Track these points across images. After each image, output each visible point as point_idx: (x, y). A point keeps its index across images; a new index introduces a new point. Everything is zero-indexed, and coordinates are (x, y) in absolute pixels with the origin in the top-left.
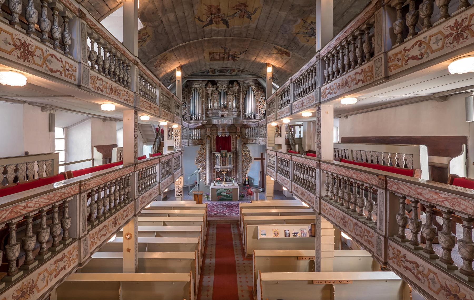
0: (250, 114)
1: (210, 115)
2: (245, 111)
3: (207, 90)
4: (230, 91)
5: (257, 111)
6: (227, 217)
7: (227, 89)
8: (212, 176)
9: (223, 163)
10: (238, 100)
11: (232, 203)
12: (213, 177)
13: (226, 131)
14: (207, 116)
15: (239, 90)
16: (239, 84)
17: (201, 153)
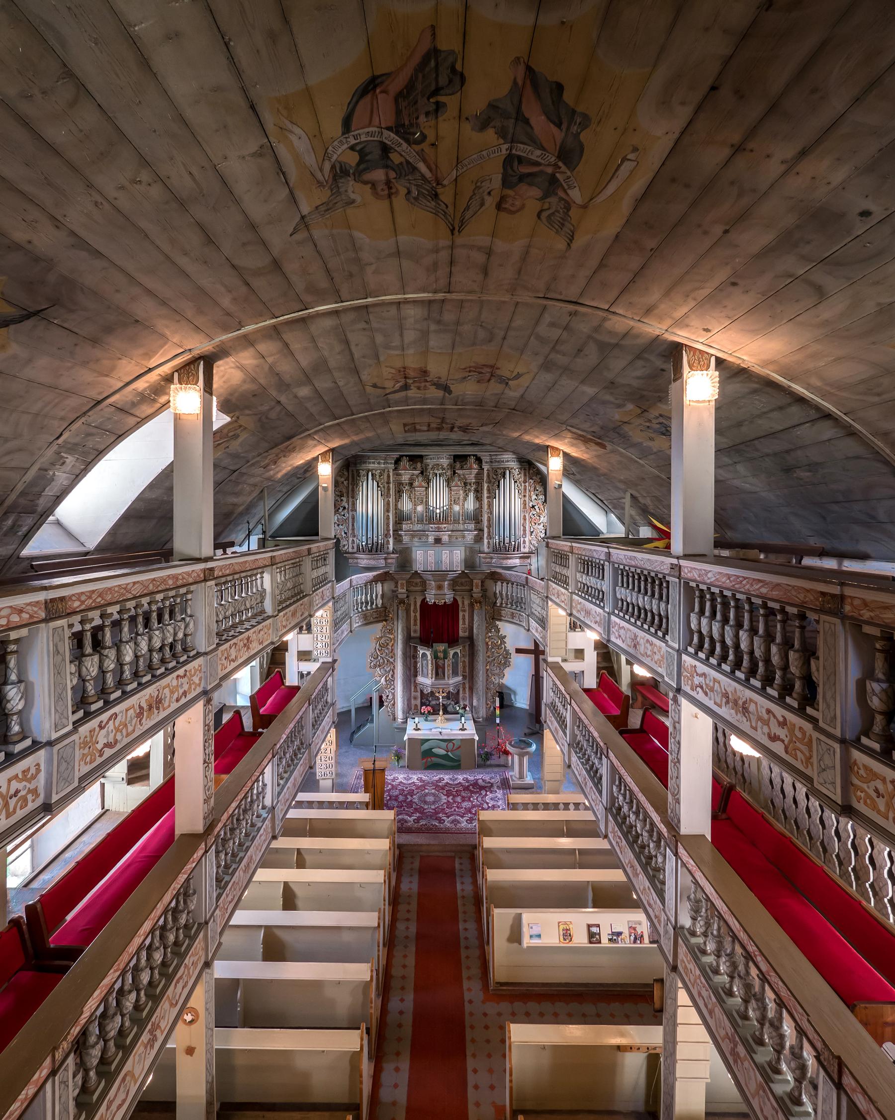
0: (507, 540)
1: (406, 539)
2: (495, 529)
3: (400, 475)
4: (456, 479)
5: (525, 530)
6: (447, 831)
7: (449, 473)
8: (409, 700)
9: (439, 672)
10: (478, 498)
11: (460, 777)
12: (413, 702)
13: (446, 591)
14: (398, 539)
15: (479, 476)
16: (479, 460)
17: (382, 641)
